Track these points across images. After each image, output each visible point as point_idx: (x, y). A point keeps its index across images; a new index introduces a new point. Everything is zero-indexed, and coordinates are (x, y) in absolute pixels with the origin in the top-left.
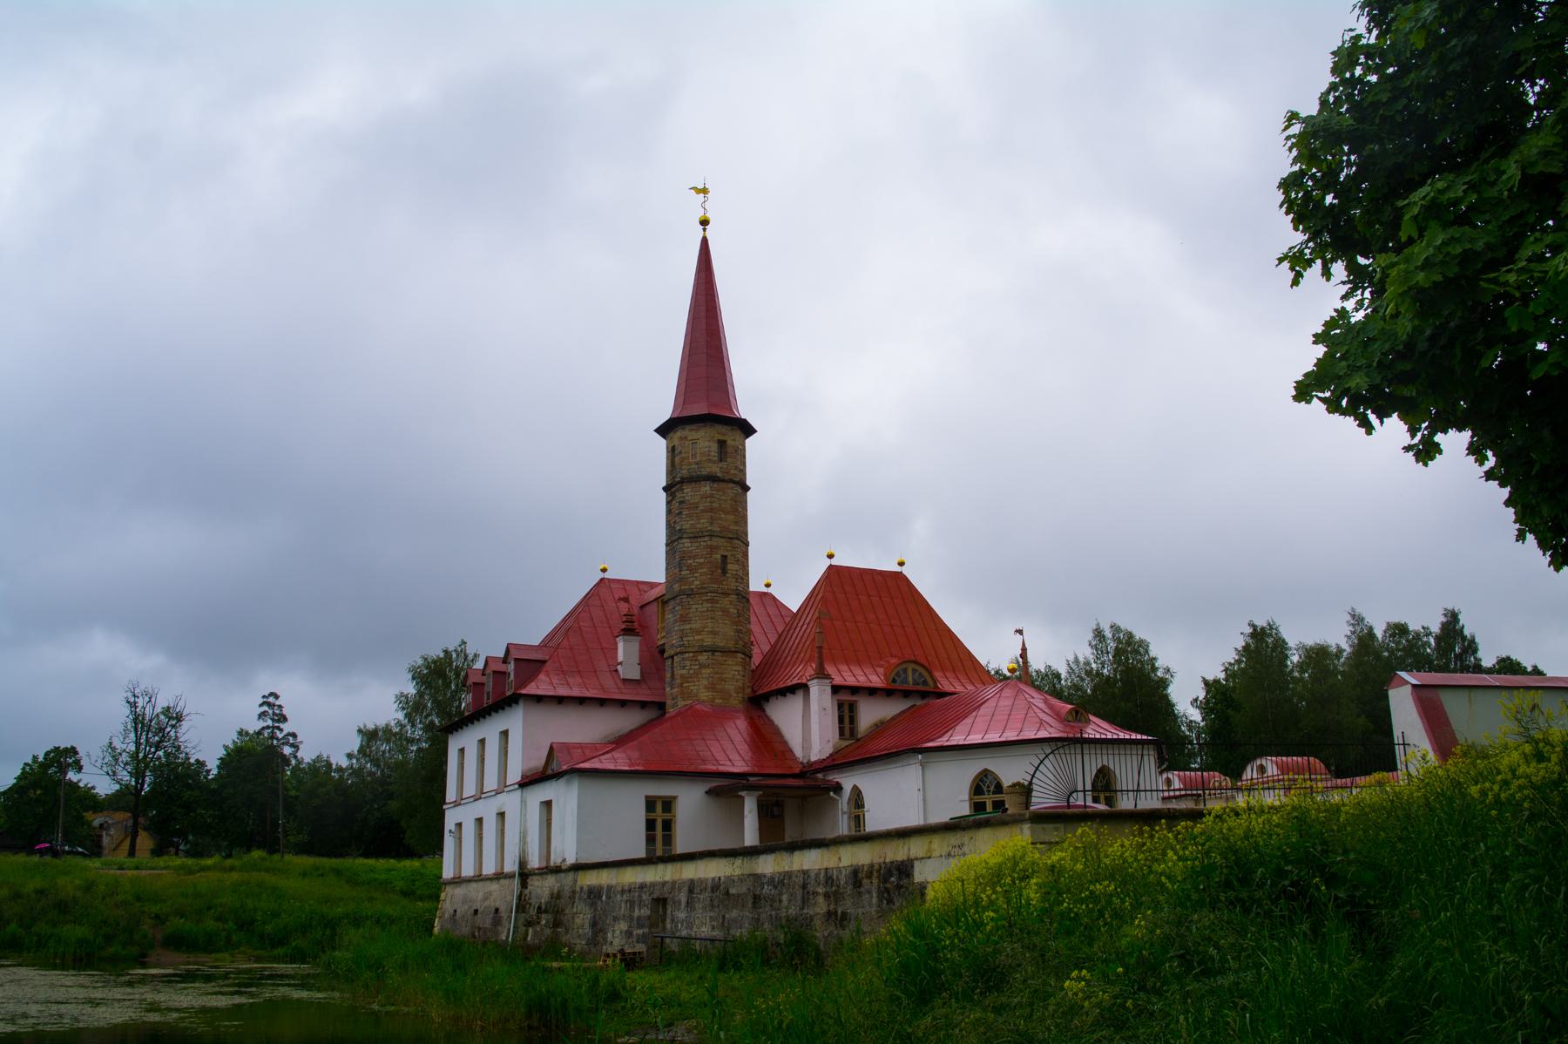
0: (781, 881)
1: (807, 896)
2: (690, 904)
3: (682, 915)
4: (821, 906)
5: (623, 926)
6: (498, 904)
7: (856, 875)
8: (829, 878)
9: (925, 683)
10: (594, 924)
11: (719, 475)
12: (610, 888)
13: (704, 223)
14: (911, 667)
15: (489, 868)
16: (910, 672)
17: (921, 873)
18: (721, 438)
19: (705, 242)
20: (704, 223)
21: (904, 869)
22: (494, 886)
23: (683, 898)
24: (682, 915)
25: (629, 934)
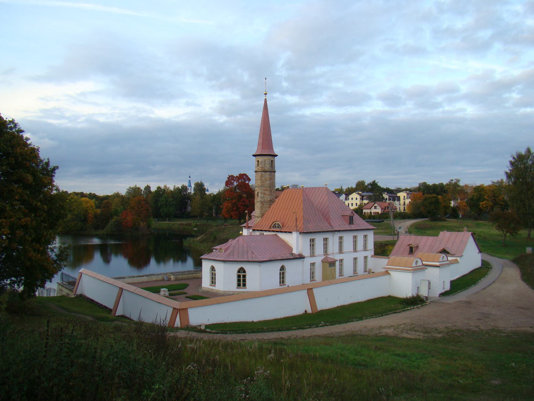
9: (281, 227)
11: (257, 170)
13: (266, 94)
14: (277, 223)
16: (277, 224)
18: (258, 160)
19: (266, 100)
20: (266, 94)
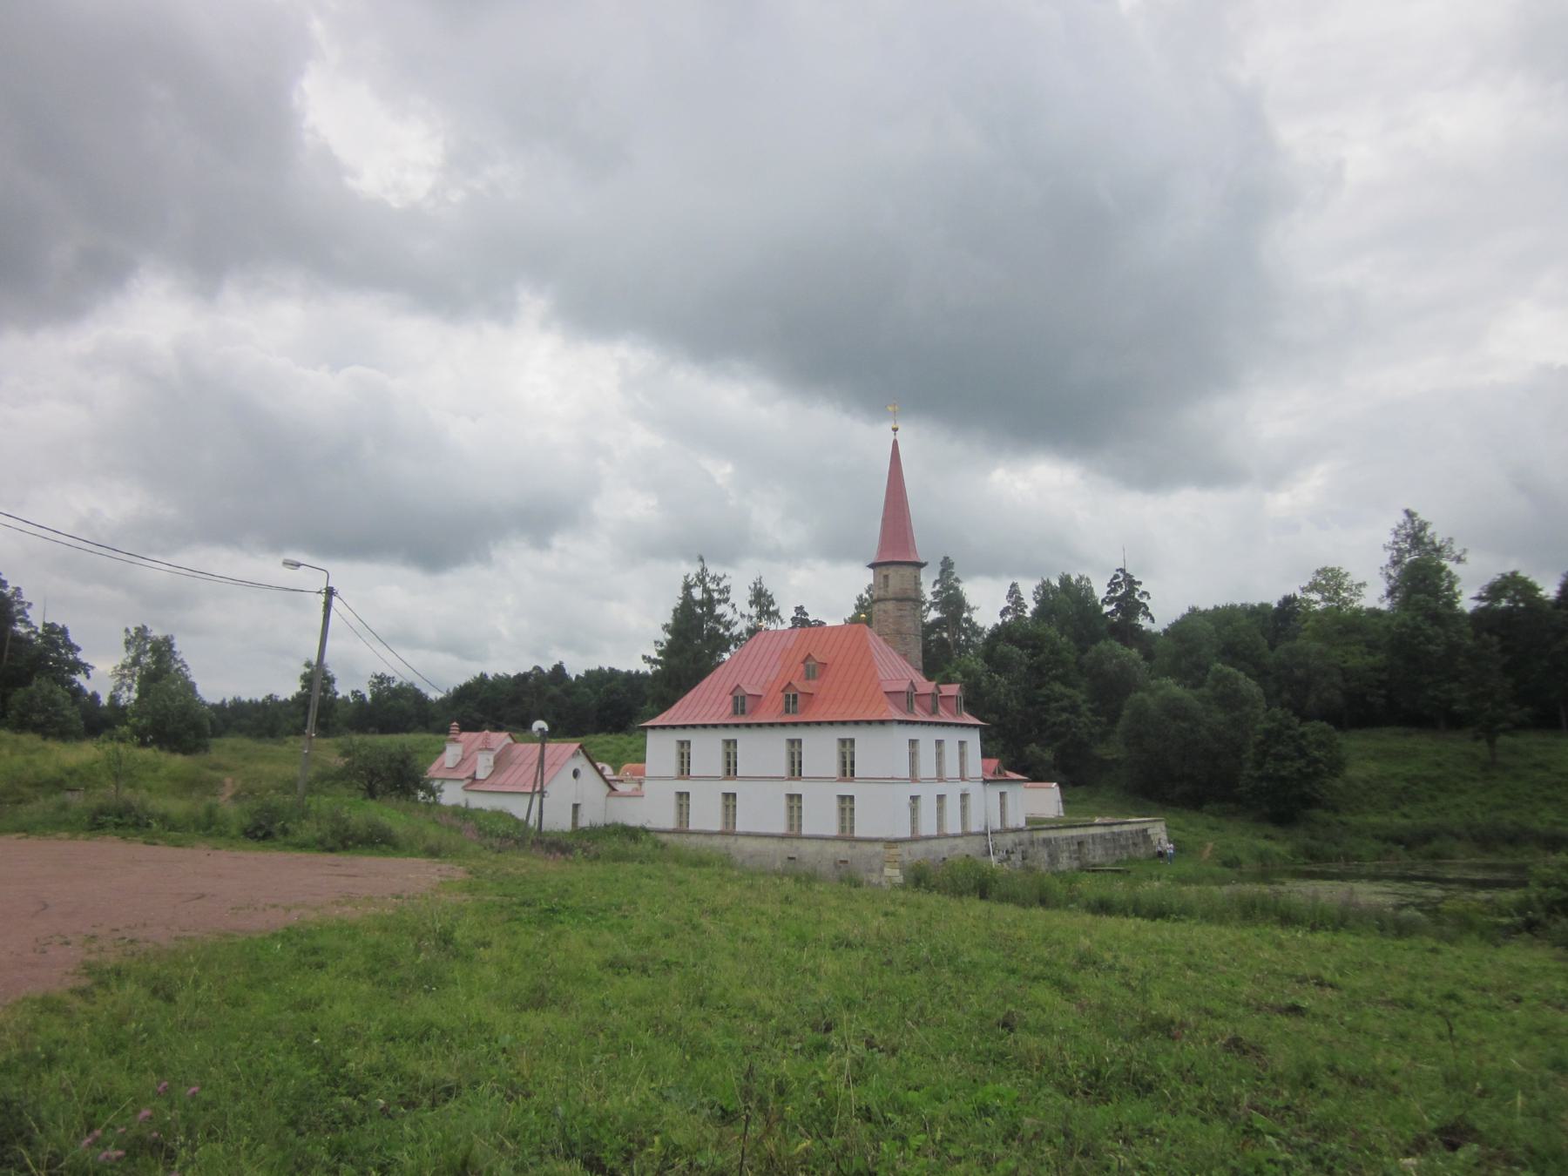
0: (1120, 834)
1: (1127, 839)
2: (1094, 843)
3: (1091, 847)
4: (1131, 842)
5: (1066, 854)
6: (967, 852)
7: (1136, 832)
8: (1131, 832)
10: (1050, 855)
12: (1055, 839)
15: (953, 826)
17: (1150, 832)
19: (895, 443)
21: (1145, 830)
22: (959, 841)
23: (1090, 841)
24: (1091, 847)
25: (1070, 857)
